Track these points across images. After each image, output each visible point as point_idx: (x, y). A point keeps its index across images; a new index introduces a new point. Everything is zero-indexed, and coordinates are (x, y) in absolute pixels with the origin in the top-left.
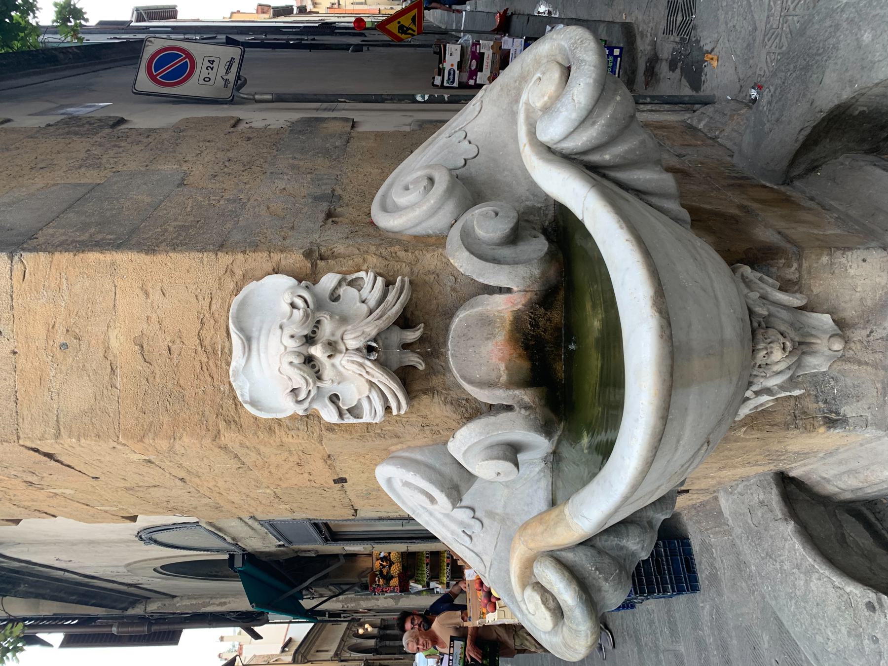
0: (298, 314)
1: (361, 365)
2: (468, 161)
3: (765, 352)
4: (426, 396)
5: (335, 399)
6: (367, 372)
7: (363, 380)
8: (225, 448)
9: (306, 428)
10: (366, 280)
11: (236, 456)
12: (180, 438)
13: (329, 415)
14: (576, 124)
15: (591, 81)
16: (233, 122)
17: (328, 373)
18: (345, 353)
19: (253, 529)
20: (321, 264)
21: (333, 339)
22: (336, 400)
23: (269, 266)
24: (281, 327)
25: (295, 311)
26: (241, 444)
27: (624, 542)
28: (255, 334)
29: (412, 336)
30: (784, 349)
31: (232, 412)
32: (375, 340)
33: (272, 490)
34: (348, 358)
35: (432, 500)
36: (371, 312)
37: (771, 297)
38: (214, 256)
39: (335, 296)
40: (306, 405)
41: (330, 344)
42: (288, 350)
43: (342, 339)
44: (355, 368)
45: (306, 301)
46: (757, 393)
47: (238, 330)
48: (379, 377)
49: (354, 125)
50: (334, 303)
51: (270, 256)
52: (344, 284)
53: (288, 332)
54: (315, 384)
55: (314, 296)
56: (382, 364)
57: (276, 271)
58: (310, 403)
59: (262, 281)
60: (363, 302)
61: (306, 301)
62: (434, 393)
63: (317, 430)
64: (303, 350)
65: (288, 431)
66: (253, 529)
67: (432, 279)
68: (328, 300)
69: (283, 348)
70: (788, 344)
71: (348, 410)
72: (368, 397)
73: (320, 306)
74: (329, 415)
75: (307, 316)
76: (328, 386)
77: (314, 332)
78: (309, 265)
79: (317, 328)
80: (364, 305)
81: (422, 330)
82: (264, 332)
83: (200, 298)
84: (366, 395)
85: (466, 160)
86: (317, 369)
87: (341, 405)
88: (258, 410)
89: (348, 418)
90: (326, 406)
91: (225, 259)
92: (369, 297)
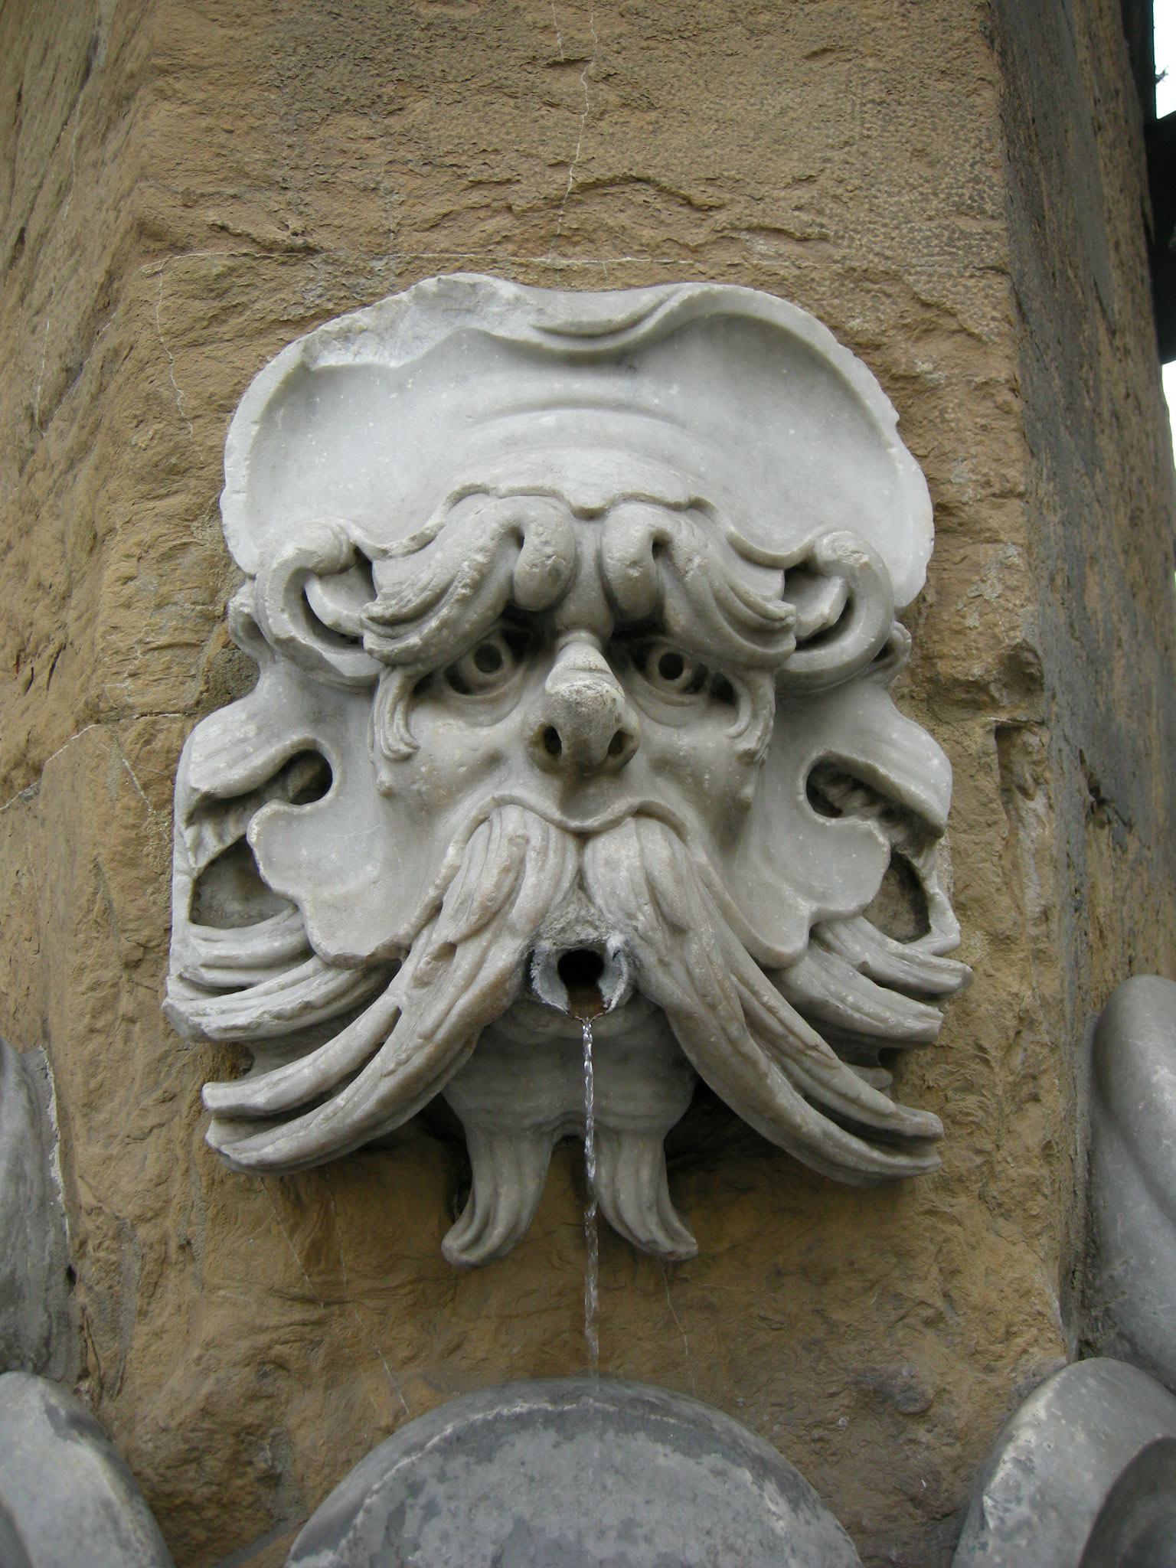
4: (298, 1260)
6: (449, 950)
7: (403, 929)
9: (164, 640)
10: (920, 949)
11: (71, 373)
18: (564, 829)
20: (978, 733)
21: (639, 763)
22: (297, 781)
23: (962, 477)
24: (696, 506)
25: (777, 580)
28: (645, 389)
31: (266, 305)
32: (637, 995)
34: (536, 840)
36: (775, 971)
38: (989, 257)
39: (833, 793)
40: (284, 624)
42: (588, 533)
43: (642, 812)
47: (671, 316)
50: (801, 784)
51: (1004, 495)
52: (900, 835)
53: (684, 533)
54: (391, 663)
55: (846, 679)
58: (288, 646)
59: (898, 449)
60: (816, 934)
62: (310, 1301)
63: (154, 695)
64: (586, 600)
65: (154, 554)
67: (919, 1290)
68: (816, 754)
69: (593, 502)
72: (306, 952)
75: (765, 629)
77: (671, 668)
78: (977, 670)
79: (694, 687)
81: (665, 1244)
82: (665, 433)
83: (804, 194)
84: (317, 938)
86: (482, 677)
87: (271, 808)
88: (272, 406)
89: (198, 844)
90: (266, 728)
92: (841, 967)
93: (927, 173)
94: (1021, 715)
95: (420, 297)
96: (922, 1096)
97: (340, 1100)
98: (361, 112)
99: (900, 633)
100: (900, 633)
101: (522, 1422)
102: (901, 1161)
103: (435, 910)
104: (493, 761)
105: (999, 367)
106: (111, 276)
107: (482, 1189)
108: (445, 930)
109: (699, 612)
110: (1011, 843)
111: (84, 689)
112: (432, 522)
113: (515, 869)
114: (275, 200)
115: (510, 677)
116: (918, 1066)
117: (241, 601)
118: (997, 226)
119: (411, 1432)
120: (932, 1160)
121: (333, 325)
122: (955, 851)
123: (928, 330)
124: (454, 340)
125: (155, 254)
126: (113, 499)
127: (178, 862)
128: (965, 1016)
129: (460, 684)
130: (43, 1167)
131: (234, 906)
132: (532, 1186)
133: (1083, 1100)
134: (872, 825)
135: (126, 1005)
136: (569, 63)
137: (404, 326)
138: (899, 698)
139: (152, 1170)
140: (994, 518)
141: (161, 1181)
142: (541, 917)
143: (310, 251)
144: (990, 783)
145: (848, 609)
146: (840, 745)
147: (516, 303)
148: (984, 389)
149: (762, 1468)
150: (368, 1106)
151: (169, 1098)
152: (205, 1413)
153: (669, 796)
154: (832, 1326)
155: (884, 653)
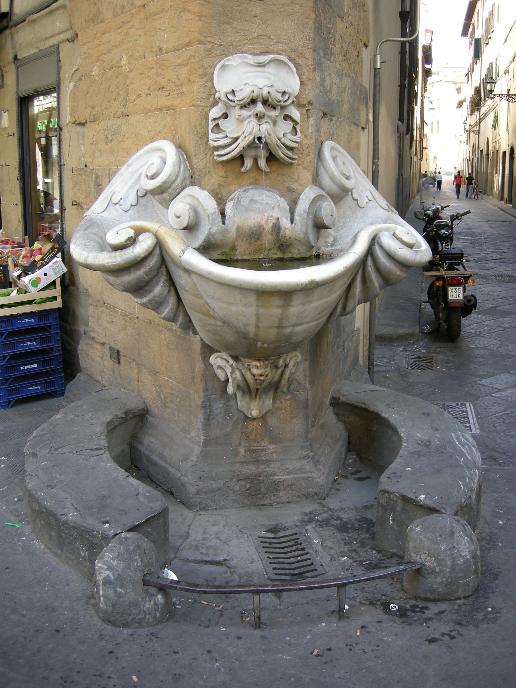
0: (279, 96)
1: (250, 134)
2: (356, 201)
3: (259, 365)
5: (225, 115)
6: (246, 137)
8: (189, 44)
10: (296, 137)
12: (200, 20)
13: (215, 112)
14: (388, 250)
15: (408, 257)
16: (367, 43)
17: (245, 113)
19: (47, 39)
20: (304, 110)
21: (266, 117)
23: (304, 78)
24: (272, 86)
26: (194, 56)
27: (161, 284)
29: (262, 163)
30: (261, 375)
31: (217, 52)
33: (125, 65)
35: (153, 177)
36: (279, 139)
37: (286, 369)
39: (286, 118)
40: (224, 99)
41: (264, 115)
43: (266, 122)
44: (249, 129)
45: (286, 101)
46: (231, 366)
48: (242, 143)
49: (363, 128)
52: (294, 123)
54: (238, 105)
56: (251, 146)
57: (302, 83)
60: (284, 135)
61: (286, 101)
63: (203, 104)
66: (47, 39)
67: (294, 177)
70: (262, 378)
71: (218, 124)
72: (227, 136)
73: (283, 108)
74: (215, 112)
75: (280, 101)
76: (235, 113)
77: (269, 105)
79: (271, 107)
80: (282, 136)
82: (268, 75)
83: (285, 37)
85: (357, 200)
87: (222, 120)
89: (212, 124)
90: (221, 110)
91: (309, 53)
92: (286, 139)
93: (302, 34)
94: (310, 108)
95: (238, 56)
96: (296, 154)
97: (233, 153)
98: (227, 24)
99: (295, 100)
100: (295, 100)
101: (251, 189)
102: (293, 161)
103: (244, 132)
104: (250, 116)
105: (310, 62)
106: (190, 42)
107: (246, 163)
108: (245, 135)
109: (273, 100)
110: (308, 124)
111: (191, 102)
112: (242, 87)
113: (253, 128)
114: (217, 38)
115: (252, 106)
116: (295, 150)
117: (217, 95)
118: (311, 42)
119: (239, 190)
120: (296, 161)
121: (227, 58)
122: (301, 126)
123: (301, 57)
124: (243, 62)
125: (201, 44)
126: (195, 77)
127: (209, 126)
128: (301, 145)
129: (245, 106)
130: (186, 164)
131: (216, 131)
132: (252, 163)
133: (316, 157)
134: (291, 122)
135: (200, 143)
136: (255, 17)
137: (236, 59)
138: (294, 106)
139: (204, 163)
140: (308, 83)
141: (206, 164)
142: (255, 133)
143: (221, 45)
144: (306, 117)
145: (289, 97)
146: (288, 113)
147: (251, 59)
148: (308, 66)
149: (277, 194)
150: (236, 154)
151: (206, 154)
152: (212, 191)
153: (269, 120)
154: (284, 181)
155: (293, 102)
